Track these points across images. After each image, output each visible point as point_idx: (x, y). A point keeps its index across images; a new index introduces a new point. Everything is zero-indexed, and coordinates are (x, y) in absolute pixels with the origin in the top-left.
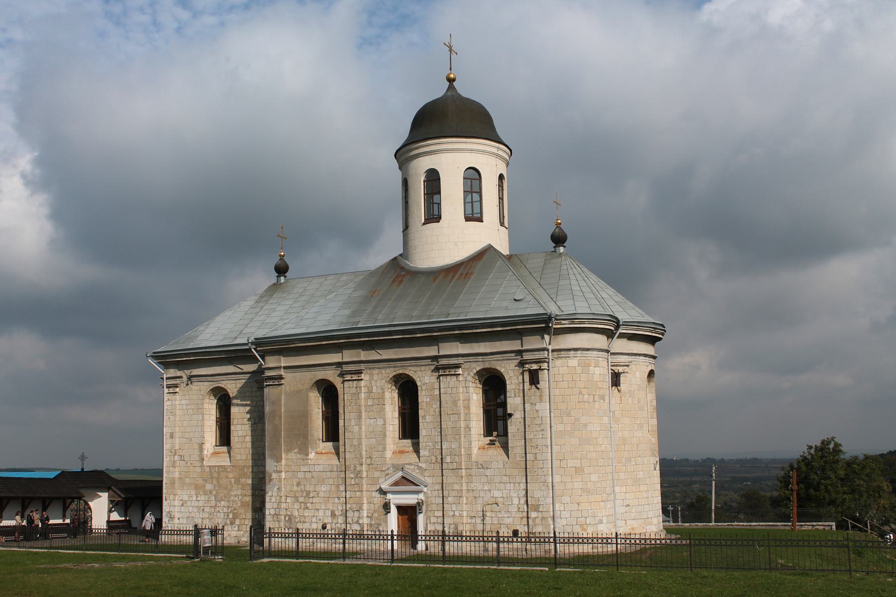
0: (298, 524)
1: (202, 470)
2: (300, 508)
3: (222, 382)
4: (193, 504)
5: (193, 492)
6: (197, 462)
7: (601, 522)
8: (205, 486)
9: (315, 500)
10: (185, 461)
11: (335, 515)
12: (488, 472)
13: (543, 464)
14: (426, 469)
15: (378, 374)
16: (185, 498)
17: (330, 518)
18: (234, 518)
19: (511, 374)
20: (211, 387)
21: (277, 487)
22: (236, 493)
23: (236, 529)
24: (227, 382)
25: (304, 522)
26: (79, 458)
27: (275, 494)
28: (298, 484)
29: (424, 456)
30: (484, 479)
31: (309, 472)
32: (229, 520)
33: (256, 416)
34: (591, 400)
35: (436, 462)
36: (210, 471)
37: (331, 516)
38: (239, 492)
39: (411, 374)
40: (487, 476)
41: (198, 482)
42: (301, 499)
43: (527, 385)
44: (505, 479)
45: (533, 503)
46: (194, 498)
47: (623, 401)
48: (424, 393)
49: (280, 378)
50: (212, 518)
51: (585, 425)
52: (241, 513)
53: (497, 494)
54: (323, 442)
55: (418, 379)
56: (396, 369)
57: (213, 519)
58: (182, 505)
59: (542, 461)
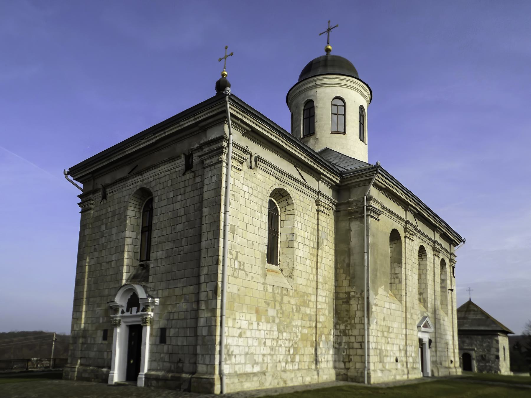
2: (385, 343)
3: (287, 186)
4: (253, 335)
5: (254, 318)
8: (267, 311)
10: (245, 271)
16: (245, 324)
18: (294, 355)
22: (297, 323)
24: (292, 189)
28: (384, 319)
32: (289, 357)
38: (299, 323)
41: (259, 305)
42: (386, 334)
50: (274, 354)
58: (240, 336)
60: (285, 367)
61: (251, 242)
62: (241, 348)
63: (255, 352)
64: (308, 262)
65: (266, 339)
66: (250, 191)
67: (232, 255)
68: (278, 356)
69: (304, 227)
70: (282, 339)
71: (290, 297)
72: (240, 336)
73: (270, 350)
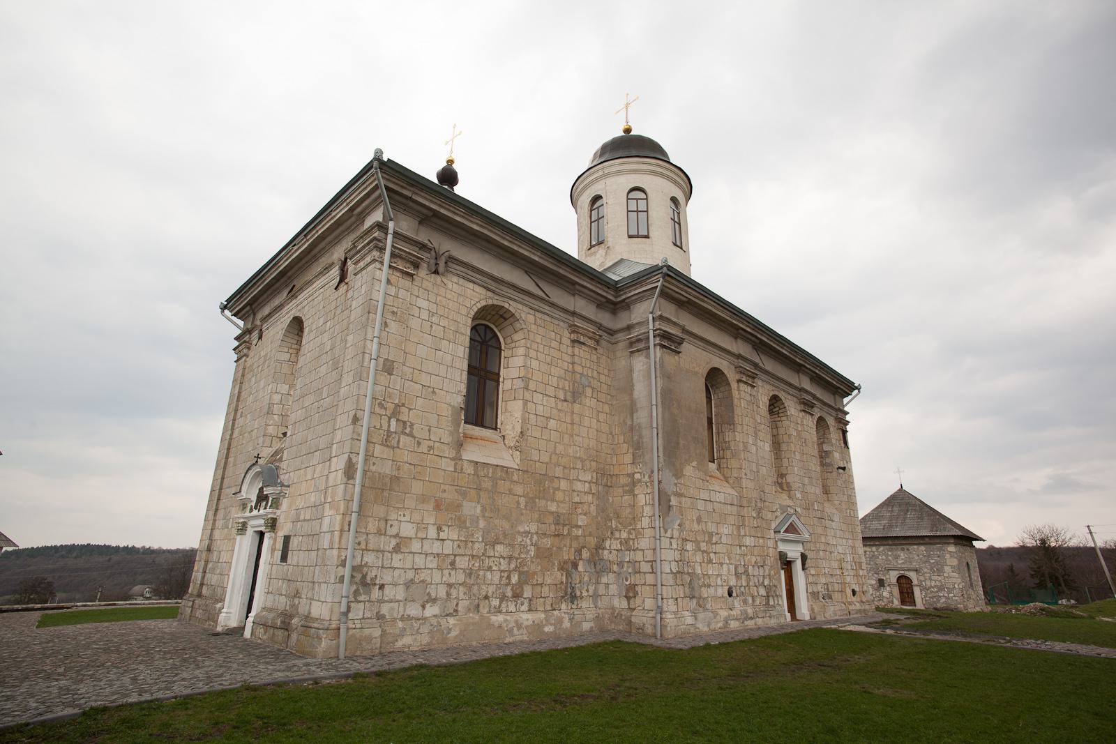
1: (455, 468)
3: (511, 302)
4: (427, 548)
6: (446, 447)
8: (460, 506)
16: (407, 530)
18: (521, 583)
20: (490, 302)
21: (678, 522)
22: (527, 529)
23: (525, 607)
24: (520, 306)
25: (709, 586)
27: (676, 534)
28: (699, 520)
31: (710, 501)
32: (509, 588)
36: (476, 474)
39: (782, 398)
41: (445, 495)
42: (703, 546)
46: (432, 532)
49: (680, 342)
52: (535, 573)
57: (476, 587)
58: (397, 549)
60: (500, 606)
61: (430, 390)
62: (397, 572)
63: (429, 580)
64: (552, 424)
65: (455, 556)
66: (433, 308)
67: (386, 409)
69: (544, 368)
70: (494, 557)
71: (512, 481)
72: (397, 549)
73: (466, 577)
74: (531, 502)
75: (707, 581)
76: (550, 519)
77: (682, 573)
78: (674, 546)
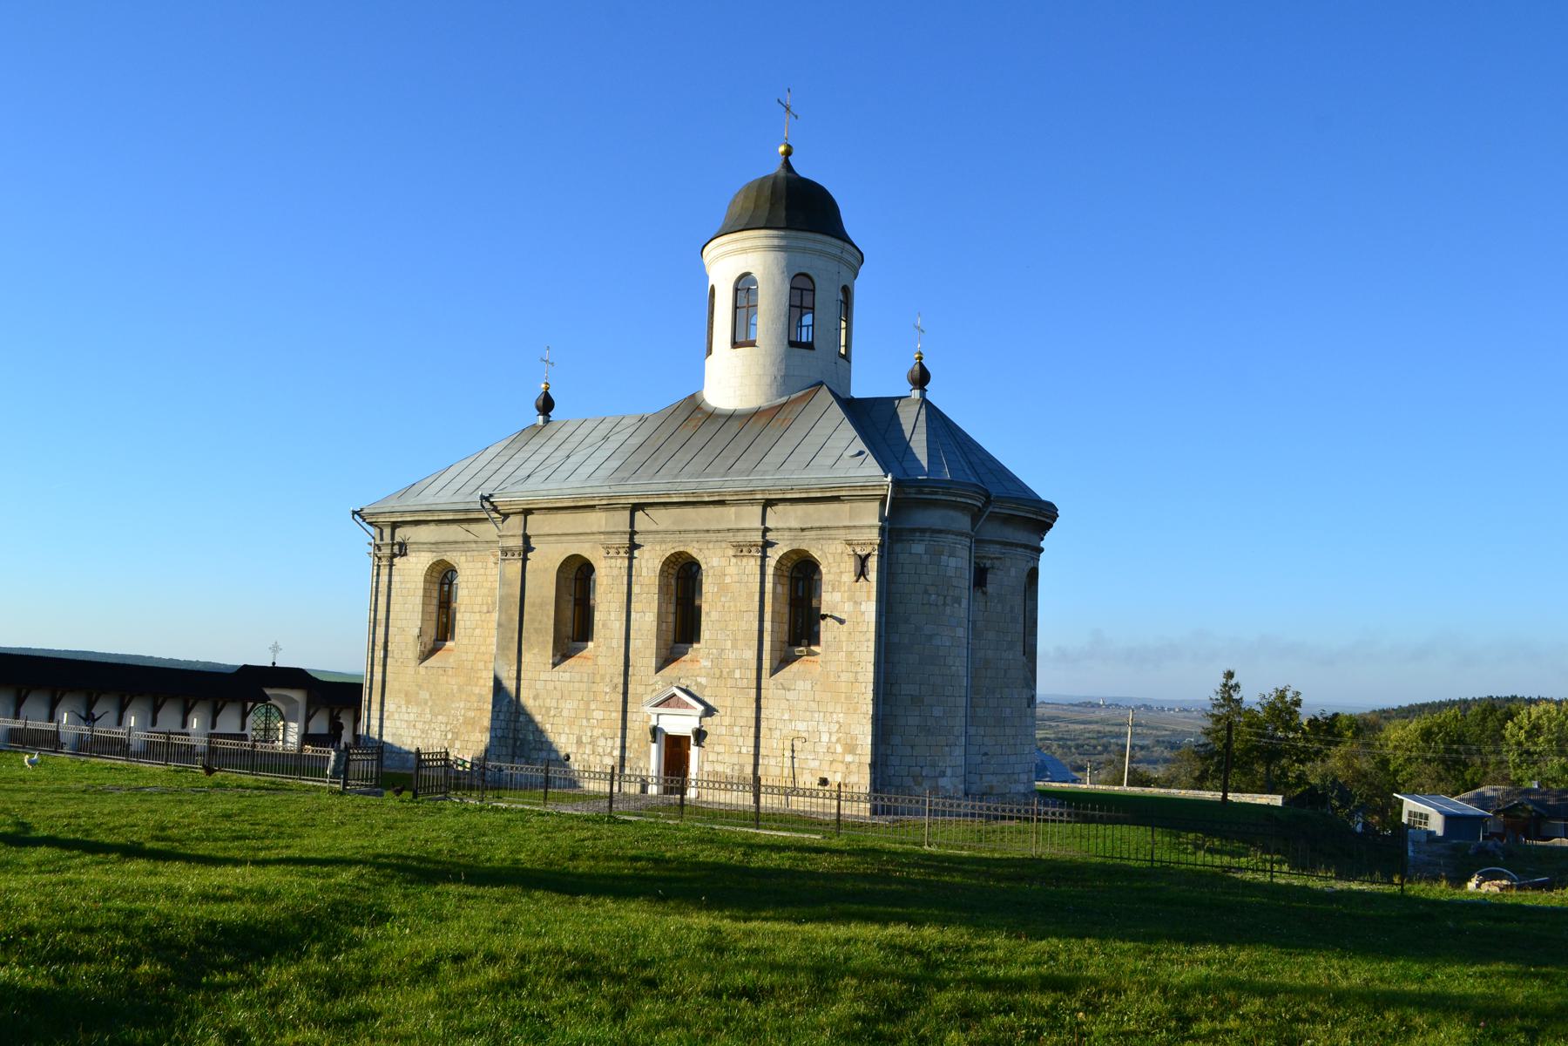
0: (533, 752)
3: (448, 554)
7: (943, 774)
8: (418, 693)
9: (556, 720)
11: (582, 742)
12: (790, 695)
13: (866, 688)
14: (706, 687)
15: (650, 551)
17: (574, 746)
19: (831, 560)
20: (435, 560)
25: (541, 750)
26: (270, 648)
27: (504, 709)
29: (705, 667)
30: (784, 705)
33: (490, 602)
34: (941, 602)
35: (721, 676)
37: (577, 743)
40: (788, 700)
43: (849, 577)
44: (814, 705)
45: (849, 741)
46: (404, 709)
47: (988, 608)
48: (710, 579)
51: (930, 637)
53: (801, 726)
54: (573, 641)
55: (704, 561)
56: (674, 545)
59: (864, 684)
64: (477, 632)
68: (431, 739)
71: (448, 676)
74: (460, 690)
75: (539, 746)
76: (474, 698)
77: (506, 738)
78: (502, 717)
